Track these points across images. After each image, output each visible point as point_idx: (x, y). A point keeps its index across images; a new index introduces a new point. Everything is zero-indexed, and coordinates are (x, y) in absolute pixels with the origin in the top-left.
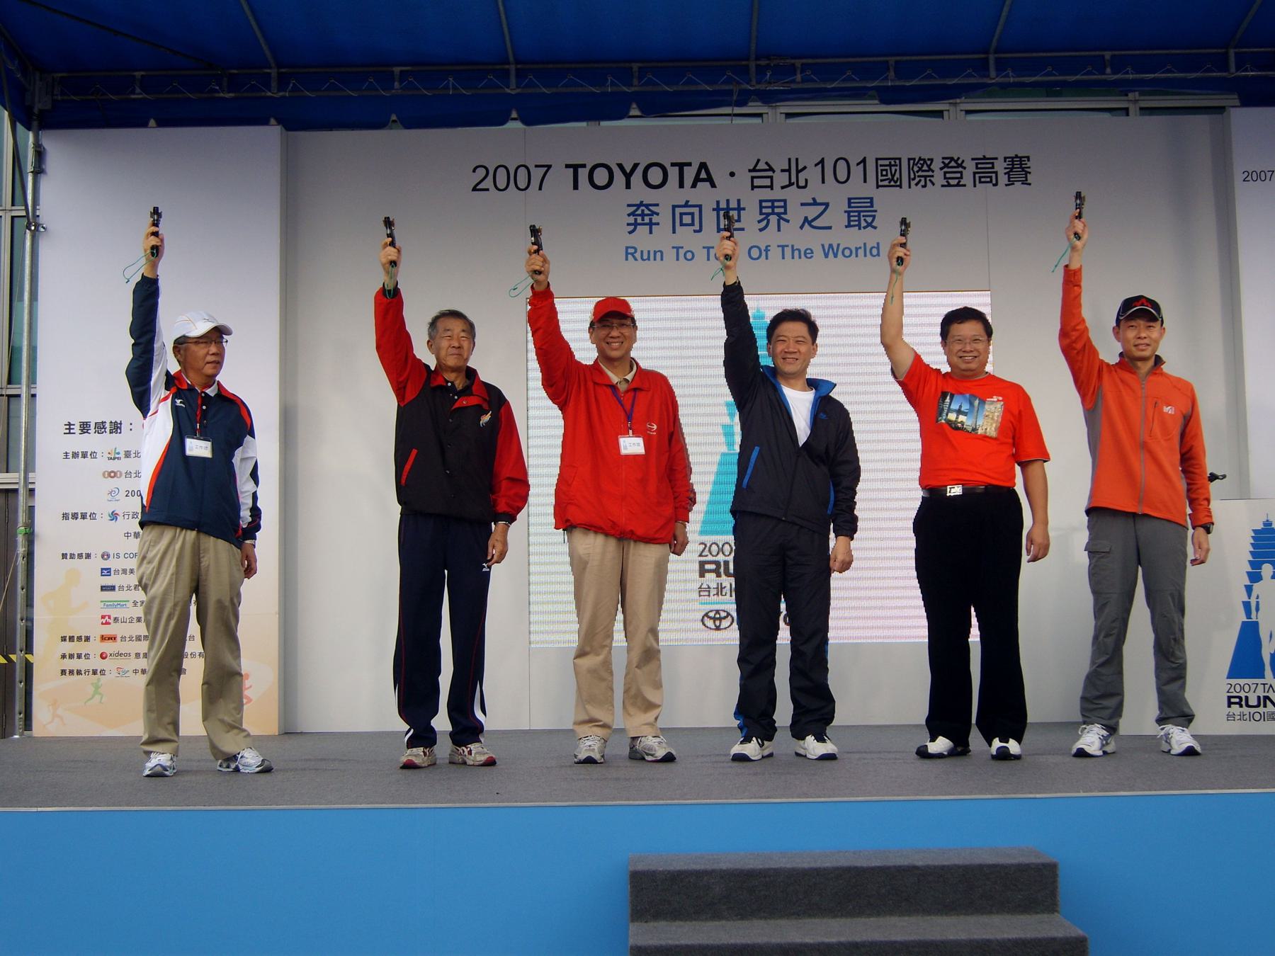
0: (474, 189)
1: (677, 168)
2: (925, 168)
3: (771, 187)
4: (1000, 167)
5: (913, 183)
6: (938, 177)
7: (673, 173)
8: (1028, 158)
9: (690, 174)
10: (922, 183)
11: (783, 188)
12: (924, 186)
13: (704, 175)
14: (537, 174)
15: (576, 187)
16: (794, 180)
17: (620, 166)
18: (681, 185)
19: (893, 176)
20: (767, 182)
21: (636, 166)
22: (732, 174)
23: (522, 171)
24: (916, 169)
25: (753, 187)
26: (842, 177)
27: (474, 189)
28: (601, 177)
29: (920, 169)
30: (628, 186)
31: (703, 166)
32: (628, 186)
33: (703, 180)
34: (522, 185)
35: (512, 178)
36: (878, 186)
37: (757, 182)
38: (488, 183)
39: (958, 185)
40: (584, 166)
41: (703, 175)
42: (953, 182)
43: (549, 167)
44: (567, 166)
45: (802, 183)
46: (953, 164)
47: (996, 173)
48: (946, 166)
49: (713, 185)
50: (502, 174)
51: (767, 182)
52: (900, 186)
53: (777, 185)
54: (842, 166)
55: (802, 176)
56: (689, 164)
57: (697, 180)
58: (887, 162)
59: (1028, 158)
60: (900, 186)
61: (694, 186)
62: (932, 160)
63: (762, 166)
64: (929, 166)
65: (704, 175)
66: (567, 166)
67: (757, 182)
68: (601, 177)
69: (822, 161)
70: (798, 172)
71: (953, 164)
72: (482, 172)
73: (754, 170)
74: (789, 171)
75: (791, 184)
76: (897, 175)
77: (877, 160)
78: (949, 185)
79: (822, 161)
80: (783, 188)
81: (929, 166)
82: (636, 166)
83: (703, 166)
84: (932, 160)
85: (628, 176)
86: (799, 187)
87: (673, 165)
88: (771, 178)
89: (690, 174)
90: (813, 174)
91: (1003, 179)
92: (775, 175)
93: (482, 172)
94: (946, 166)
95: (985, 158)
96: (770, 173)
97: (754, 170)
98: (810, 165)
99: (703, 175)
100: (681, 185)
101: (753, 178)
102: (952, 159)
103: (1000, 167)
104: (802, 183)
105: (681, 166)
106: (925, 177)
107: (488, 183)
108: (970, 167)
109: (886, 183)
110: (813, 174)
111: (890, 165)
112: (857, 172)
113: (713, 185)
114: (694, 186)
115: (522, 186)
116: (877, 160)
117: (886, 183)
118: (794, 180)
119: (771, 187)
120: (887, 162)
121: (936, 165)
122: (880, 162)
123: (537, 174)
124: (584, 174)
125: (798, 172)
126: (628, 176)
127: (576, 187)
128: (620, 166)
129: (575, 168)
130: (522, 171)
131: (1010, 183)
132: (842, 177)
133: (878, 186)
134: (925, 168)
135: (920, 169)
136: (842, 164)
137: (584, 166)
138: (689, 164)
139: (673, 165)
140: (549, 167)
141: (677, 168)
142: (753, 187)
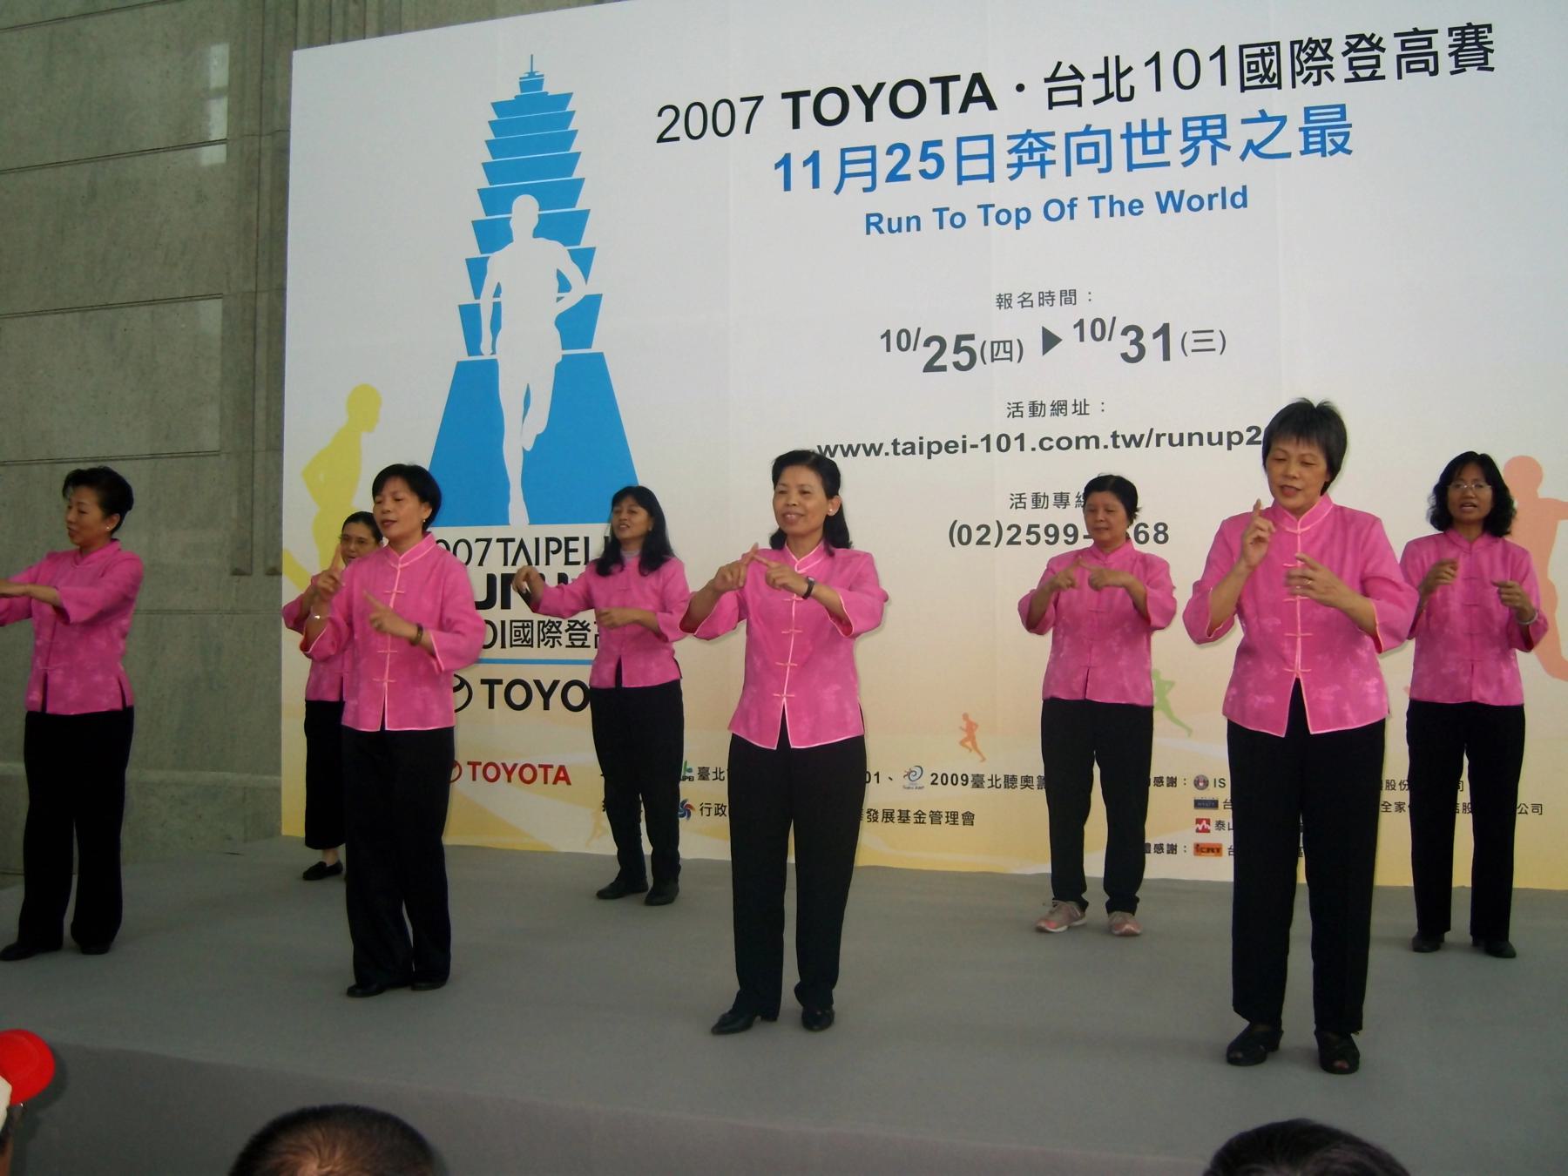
0: (661, 140)
1: (939, 86)
2: (1319, 54)
3: (1079, 102)
4: (1442, 44)
5: (1299, 79)
6: (1340, 67)
7: (933, 92)
8: (1489, 27)
9: (957, 92)
10: (1314, 78)
11: (1096, 102)
12: (1318, 83)
13: (979, 92)
14: (743, 110)
15: (796, 125)
16: (1113, 88)
17: (858, 89)
18: (945, 110)
19: (1267, 70)
20: (1073, 95)
21: (880, 86)
22: (1020, 88)
23: (724, 110)
24: (1303, 57)
25: (1051, 105)
26: (1187, 76)
27: (661, 140)
28: (831, 106)
29: (1311, 57)
30: (869, 117)
31: (977, 79)
32: (869, 117)
33: (978, 100)
34: (723, 128)
35: (710, 119)
36: (1243, 89)
37: (1057, 96)
38: (678, 130)
39: (1372, 77)
40: (807, 93)
41: (977, 92)
42: (1367, 73)
43: (759, 99)
44: (785, 96)
45: (1125, 93)
46: (1364, 45)
47: (1435, 54)
48: (1353, 48)
49: (992, 106)
50: (696, 111)
51: (1073, 95)
52: (1279, 86)
53: (1087, 99)
54: (1187, 62)
55: (1126, 82)
56: (957, 78)
57: (968, 99)
58: (1257, 50)
59: (1489, 27)
60: (1279, 86)
61: (964, 109)
62: (1329, 41)
63: (1065, 71)
64: (1324, 51)
65: (979, 92)
66: (785, 96)
67: (1057, 96)
68: (831, 106)
69: (1156, 58)
70: (1119, 76)
71: (1364, 45)
72: (670, 114)
73: (1053, 78)
74: (1105, 75)
75: (1108, 96)
76: (1274, 69)
77: (1242, 48)
78: (1357, 79)
79: (1156, 58)
80: (1096, 102)
81: (1324, 51)
82: (880, 86)
83: (977, 79)
84: (1329, 41)
85: (869, 103)
86: (1120, 99)
87: (933, 80)
88: (1079, 88)
89: (957, 92)
90: (1142, 78)
91: (1447, 63)
92: (1084, 85)
93: (670, 114)
94: (1353, 48)
95: (1416, 31)
96: (1076, 82)
97: (1053, 78)
98: (1139, 67)
99: (977, 92)
100: (945, 110)
101: (1051, 91)
102: (1361, 37)
103: (1442, 44)
104: (1125, 93)
105: (945, 81)
106: (1319, 68)
107: (678, 130)
108: (1393, 47)
109: (1256, 82)
110: (1142, 78)
111: (1263, 55)
112: (1211, 69)
113: (992, 106)
114: (964, 109)
115: (723, 126)
116: (1242, 48)
117: (1256, 82)
118: (1113, 88)
119: (1079, 102)
120: (1257, 50)
121: (1337, 49)
122: (1246, 51)
123: (743, 110)
124: (806, 104)
125: (1119, 76)
126: (869, 103)
127: (796, 125)
128: (858, 89)
129: (795, 97)
130: (724, 110)
131: (1460, 69)
132: (1187, 81)
133: (1243, 89)
134: (1319, 54)
135: (1311, 57)
136: (1187, 62)
137: (807, 93)
138: (957, 78)
139: (933, 80)
140: (759, 99)
141: (939, 86)
142: (1051, 105)
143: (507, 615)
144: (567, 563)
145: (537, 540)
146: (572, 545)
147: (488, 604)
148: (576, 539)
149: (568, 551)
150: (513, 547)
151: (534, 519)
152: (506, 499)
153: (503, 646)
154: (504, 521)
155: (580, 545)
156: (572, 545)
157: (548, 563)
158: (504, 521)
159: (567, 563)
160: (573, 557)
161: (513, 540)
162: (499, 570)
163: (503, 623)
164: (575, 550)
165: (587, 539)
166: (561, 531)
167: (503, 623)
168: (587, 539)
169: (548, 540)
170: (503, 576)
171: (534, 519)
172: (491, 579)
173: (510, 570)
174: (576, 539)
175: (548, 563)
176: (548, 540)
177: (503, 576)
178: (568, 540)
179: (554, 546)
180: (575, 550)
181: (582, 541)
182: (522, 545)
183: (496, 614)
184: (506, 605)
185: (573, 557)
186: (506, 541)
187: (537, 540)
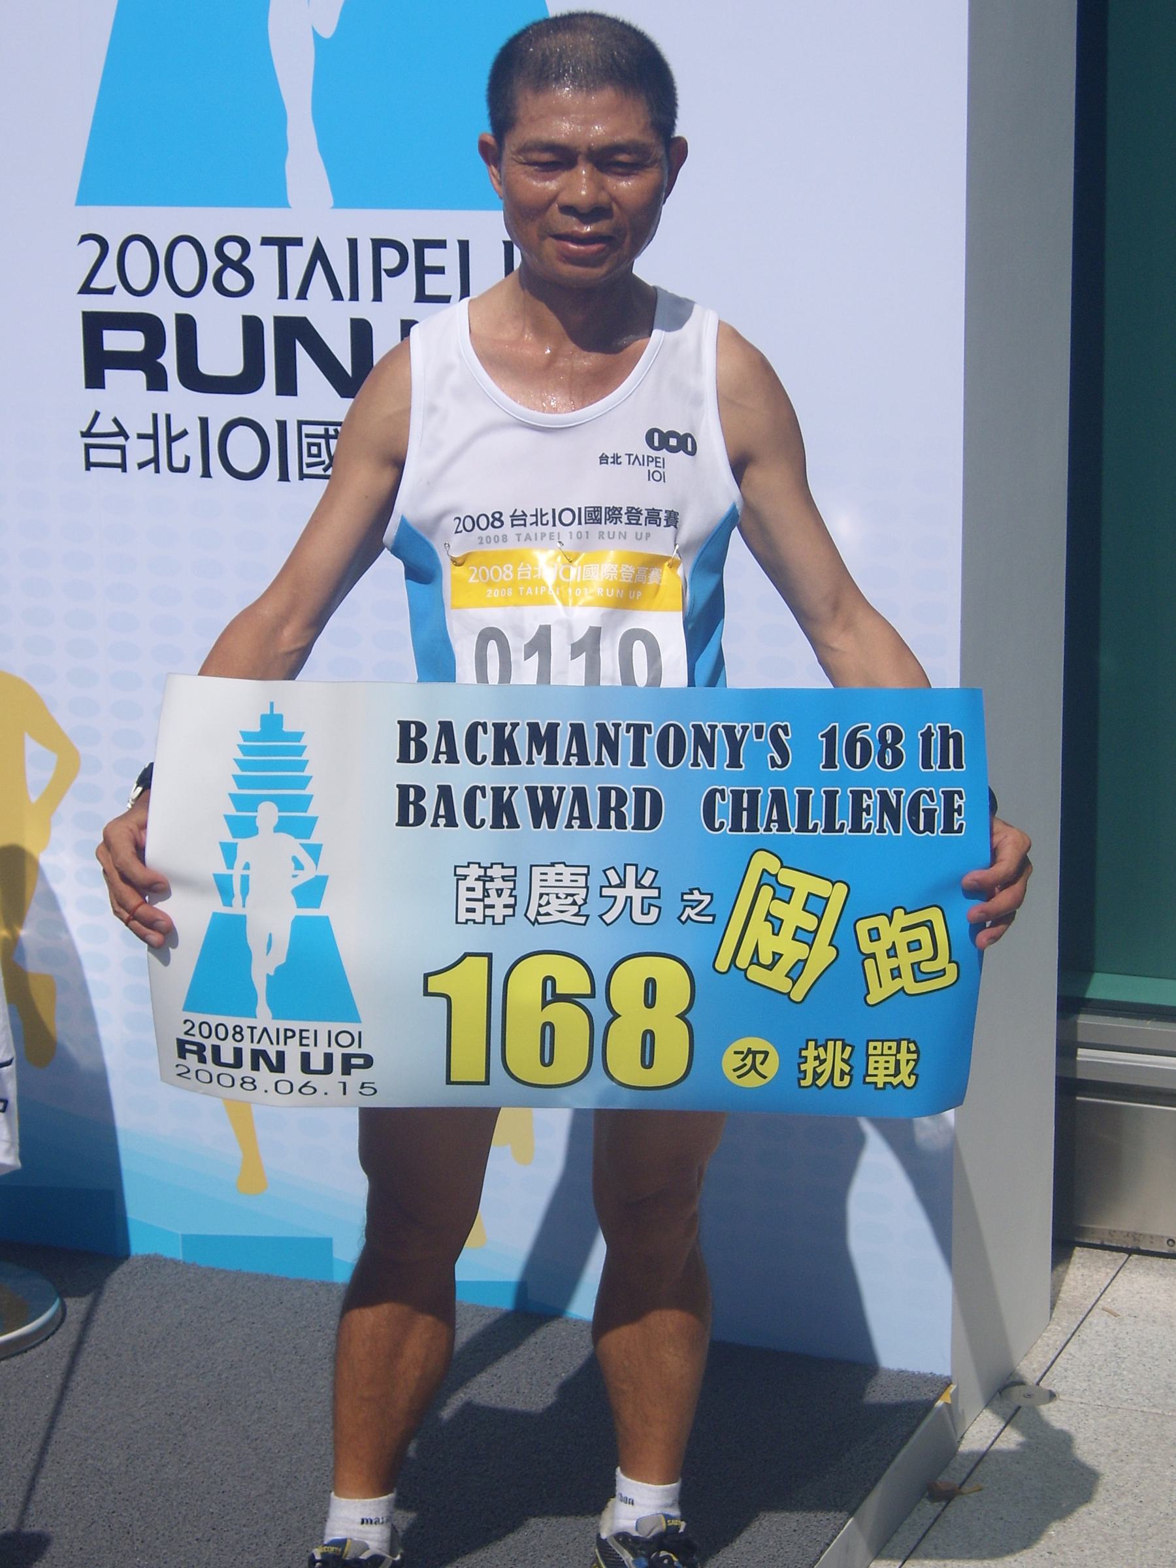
143: (290, 409)
144: (422, 297)
145: (353, 244)
146: (432, 257)
147: (248, 382)
148: (441, 244)
149: (422, 271)
150: (298, 259)
151: (347, 194)
152: (282, 149)
153: (284, 476)
154: (276, 197)
155: (448, 258)
156: (432, 257)
157: (378, 297)
158: (276, 197)
159: (422, 297)
160: (433, 284)
161: (298, 242)
162: (266, 305)
163: (282, 426)
164: (440, 270)
165: (464, 246)
166: (407, 226)
167: (282, 426)
168: (464, 246)
169: (378, 244)
170: (279, 322)
171: (347, 194)
172: (252, 326)
173: (292, 308)
174: (441, 244)
175: (378, 297)
176: (378, 244)
177: (279, 322)
178: (421, 245)
179: (390, 258)
180: (440, 270)
181: (453, 250)
182: (319, 254)
183: (265, 404)
184: (287, 385)
185: (433, 284)
186: (282, 244)
187: (353, 244)
